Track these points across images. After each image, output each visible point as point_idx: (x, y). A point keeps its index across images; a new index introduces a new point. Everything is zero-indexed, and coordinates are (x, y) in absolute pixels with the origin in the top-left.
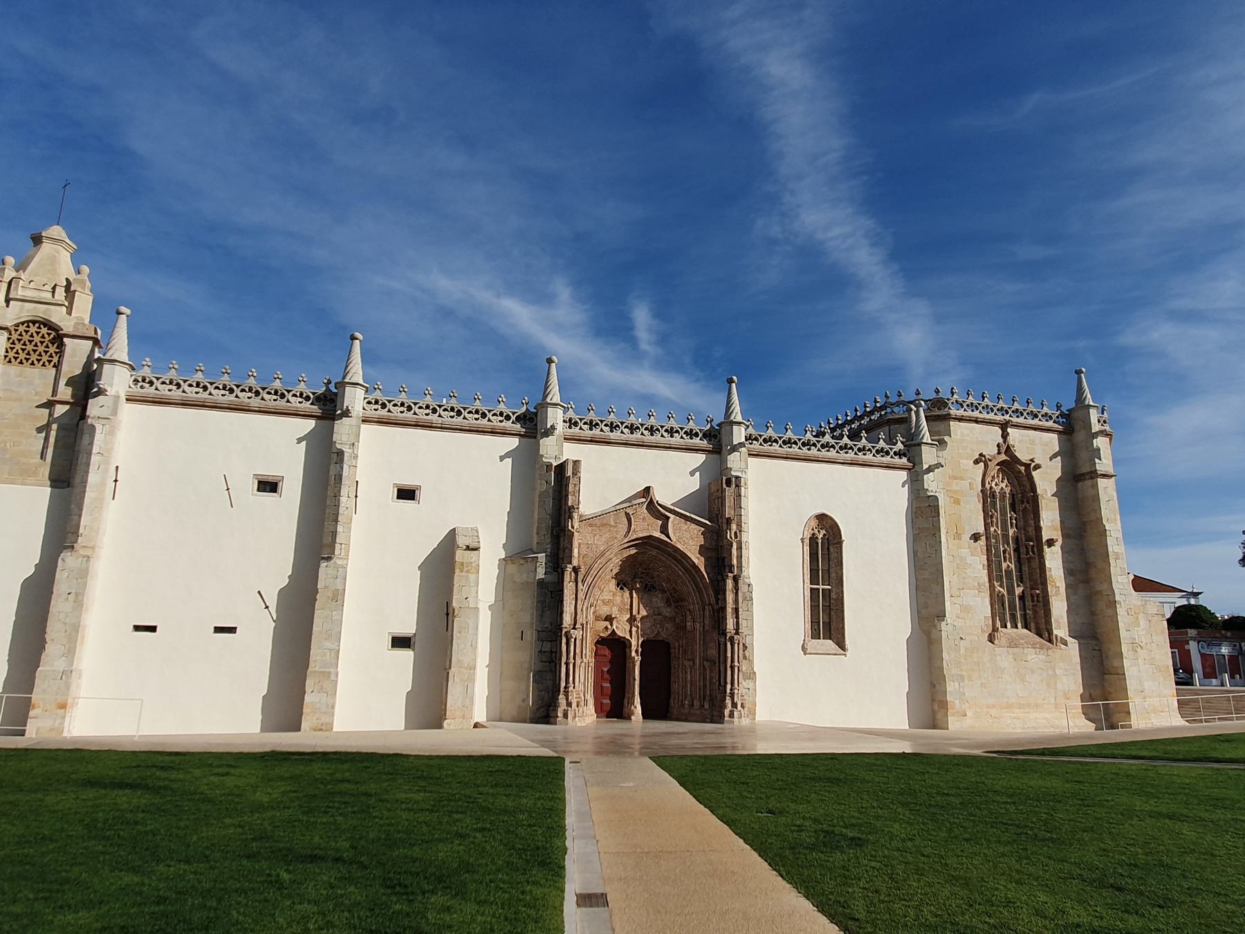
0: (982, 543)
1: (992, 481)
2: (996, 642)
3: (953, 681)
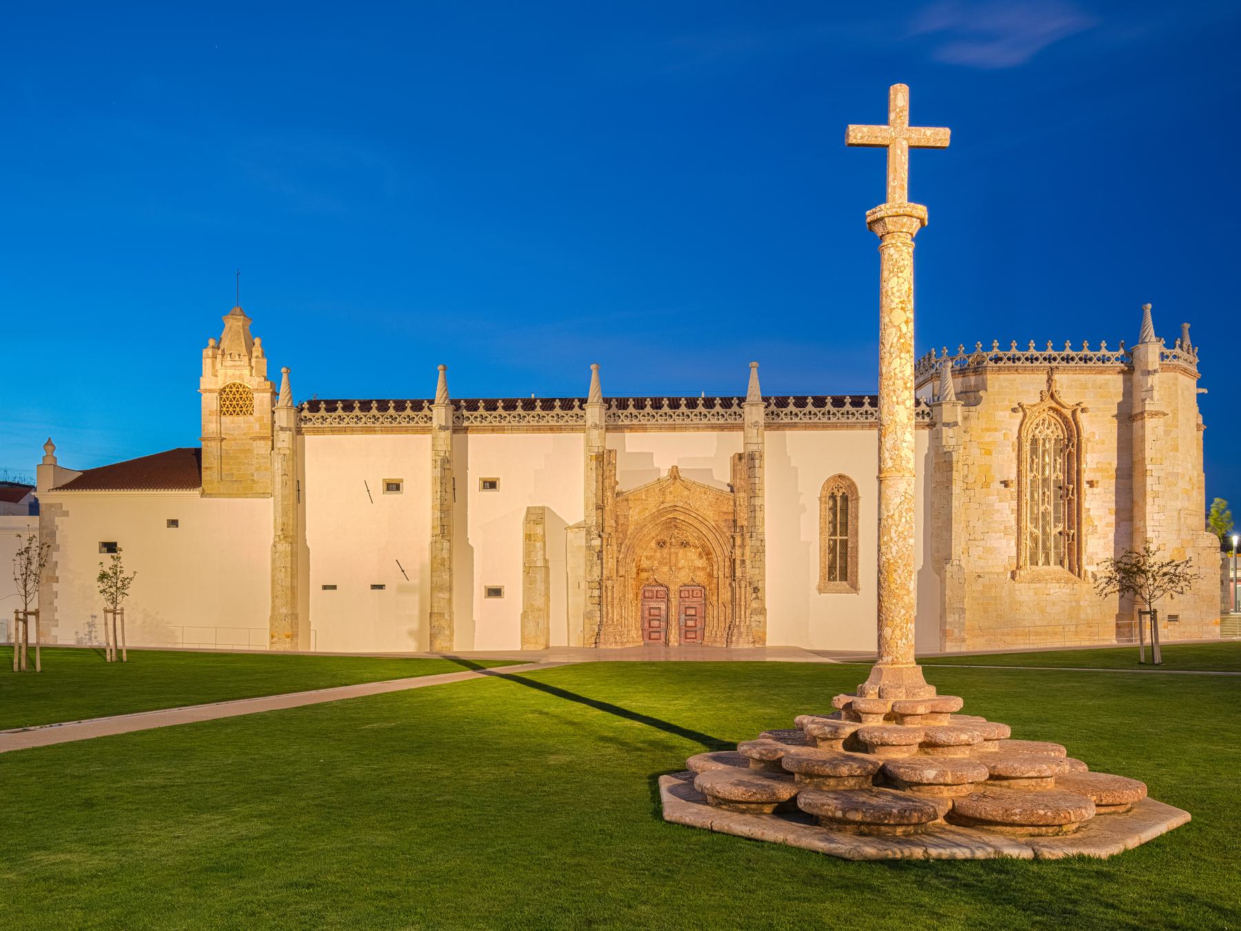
0: (1012, 490)
1: (1036, 428)
2: (1016, 579)
3: (954, 614)
